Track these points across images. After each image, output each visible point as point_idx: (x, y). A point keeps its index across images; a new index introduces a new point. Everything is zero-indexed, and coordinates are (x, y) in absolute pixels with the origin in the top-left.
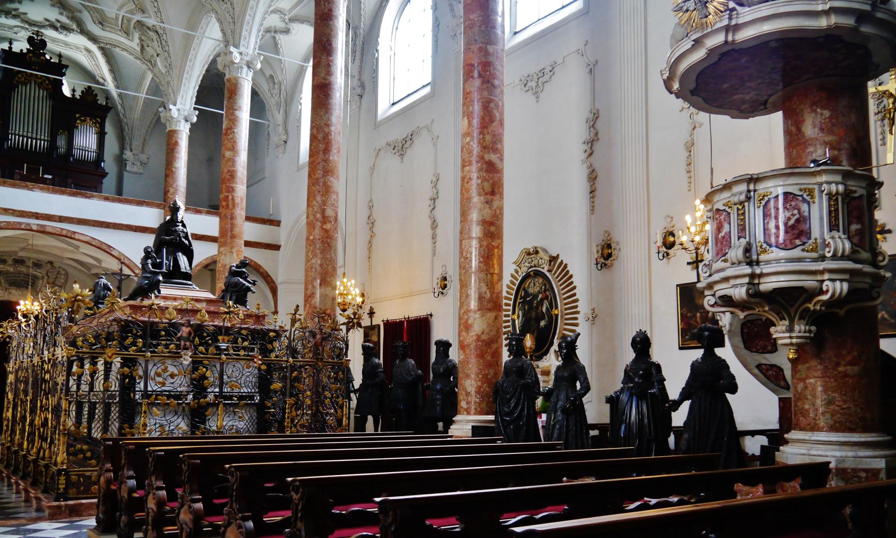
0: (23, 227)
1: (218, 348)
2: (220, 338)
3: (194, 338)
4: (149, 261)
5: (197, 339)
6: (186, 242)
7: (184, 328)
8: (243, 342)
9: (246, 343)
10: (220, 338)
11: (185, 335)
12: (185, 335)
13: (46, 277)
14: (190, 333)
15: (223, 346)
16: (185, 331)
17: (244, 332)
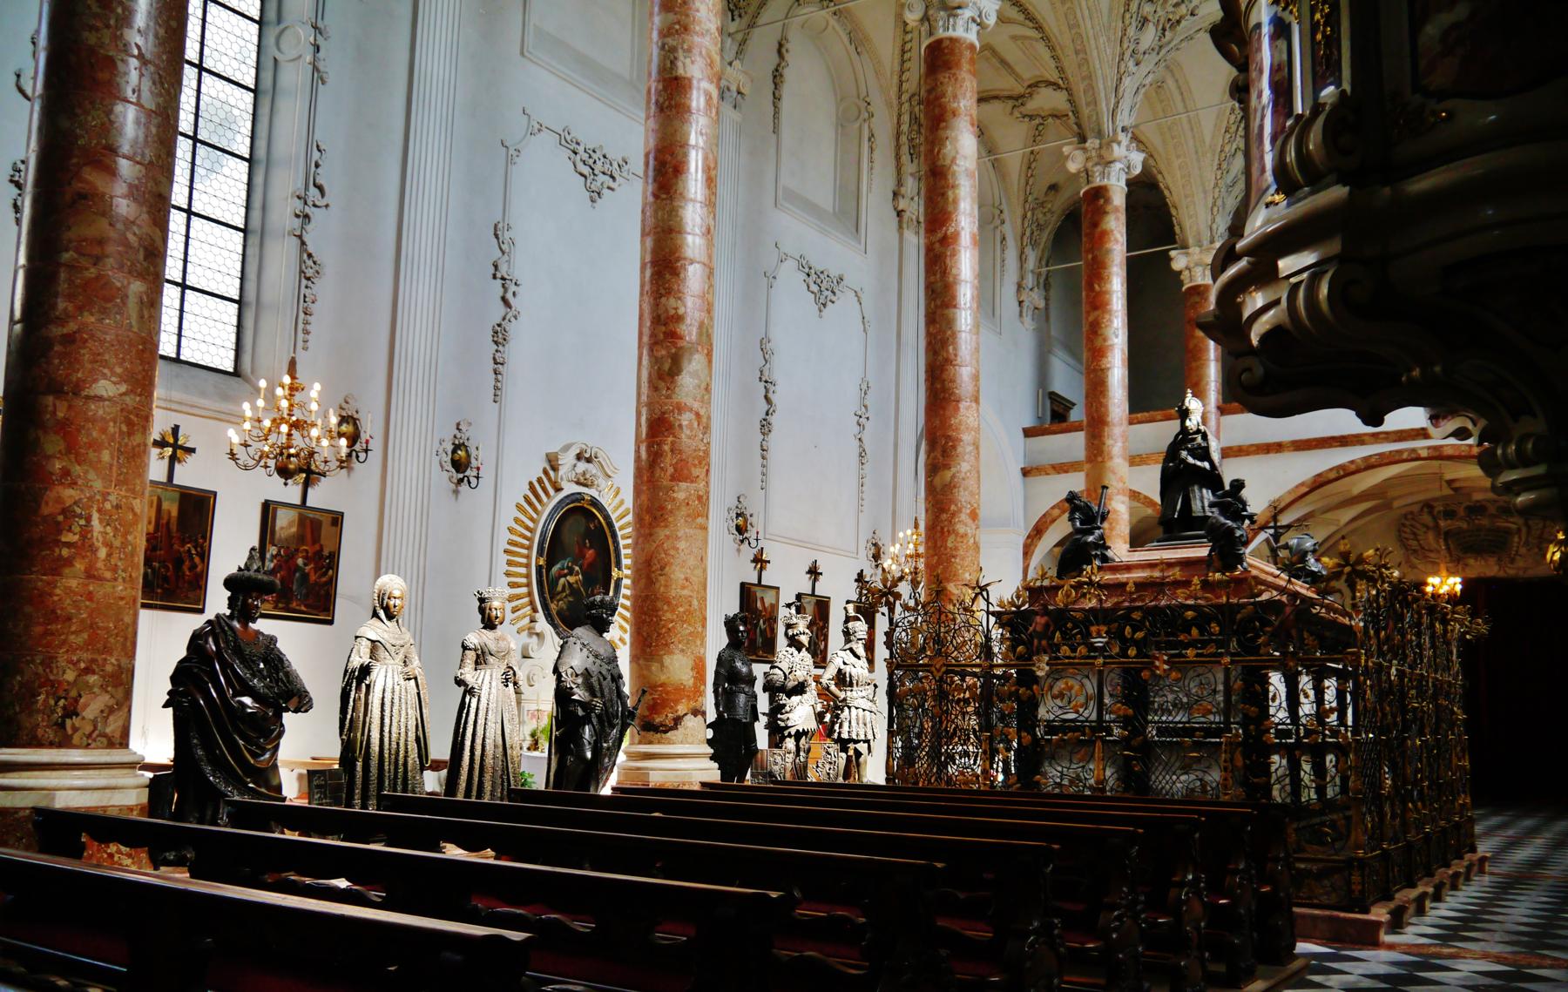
0: (1405, 456)
1: (1091, 647)
2: (1094, 629)
3: (1054, 633)
4: (1077, 515)
5: (1058, 634)
6: (1206, 465)
7: (1038, 619)
8: (1134, 632)
9: (1139, 635)
10: (1094, 629)
11: (1039, 629)
12: (1039, 629)
13: (1524, 530)
14: (1047, 626)
15: (1099, 642)
16: (1040, 621)
17: (1136, 616)
